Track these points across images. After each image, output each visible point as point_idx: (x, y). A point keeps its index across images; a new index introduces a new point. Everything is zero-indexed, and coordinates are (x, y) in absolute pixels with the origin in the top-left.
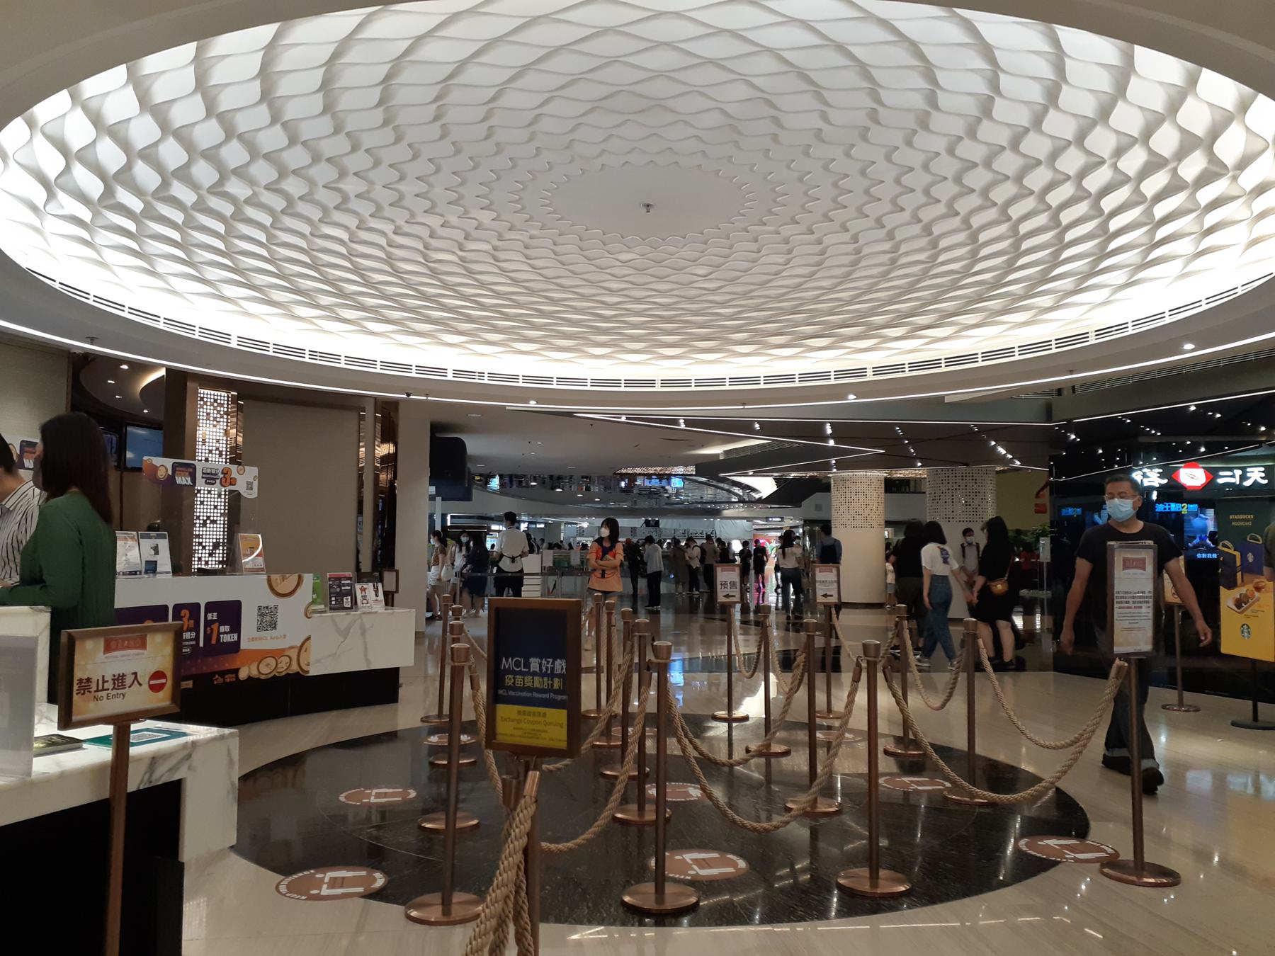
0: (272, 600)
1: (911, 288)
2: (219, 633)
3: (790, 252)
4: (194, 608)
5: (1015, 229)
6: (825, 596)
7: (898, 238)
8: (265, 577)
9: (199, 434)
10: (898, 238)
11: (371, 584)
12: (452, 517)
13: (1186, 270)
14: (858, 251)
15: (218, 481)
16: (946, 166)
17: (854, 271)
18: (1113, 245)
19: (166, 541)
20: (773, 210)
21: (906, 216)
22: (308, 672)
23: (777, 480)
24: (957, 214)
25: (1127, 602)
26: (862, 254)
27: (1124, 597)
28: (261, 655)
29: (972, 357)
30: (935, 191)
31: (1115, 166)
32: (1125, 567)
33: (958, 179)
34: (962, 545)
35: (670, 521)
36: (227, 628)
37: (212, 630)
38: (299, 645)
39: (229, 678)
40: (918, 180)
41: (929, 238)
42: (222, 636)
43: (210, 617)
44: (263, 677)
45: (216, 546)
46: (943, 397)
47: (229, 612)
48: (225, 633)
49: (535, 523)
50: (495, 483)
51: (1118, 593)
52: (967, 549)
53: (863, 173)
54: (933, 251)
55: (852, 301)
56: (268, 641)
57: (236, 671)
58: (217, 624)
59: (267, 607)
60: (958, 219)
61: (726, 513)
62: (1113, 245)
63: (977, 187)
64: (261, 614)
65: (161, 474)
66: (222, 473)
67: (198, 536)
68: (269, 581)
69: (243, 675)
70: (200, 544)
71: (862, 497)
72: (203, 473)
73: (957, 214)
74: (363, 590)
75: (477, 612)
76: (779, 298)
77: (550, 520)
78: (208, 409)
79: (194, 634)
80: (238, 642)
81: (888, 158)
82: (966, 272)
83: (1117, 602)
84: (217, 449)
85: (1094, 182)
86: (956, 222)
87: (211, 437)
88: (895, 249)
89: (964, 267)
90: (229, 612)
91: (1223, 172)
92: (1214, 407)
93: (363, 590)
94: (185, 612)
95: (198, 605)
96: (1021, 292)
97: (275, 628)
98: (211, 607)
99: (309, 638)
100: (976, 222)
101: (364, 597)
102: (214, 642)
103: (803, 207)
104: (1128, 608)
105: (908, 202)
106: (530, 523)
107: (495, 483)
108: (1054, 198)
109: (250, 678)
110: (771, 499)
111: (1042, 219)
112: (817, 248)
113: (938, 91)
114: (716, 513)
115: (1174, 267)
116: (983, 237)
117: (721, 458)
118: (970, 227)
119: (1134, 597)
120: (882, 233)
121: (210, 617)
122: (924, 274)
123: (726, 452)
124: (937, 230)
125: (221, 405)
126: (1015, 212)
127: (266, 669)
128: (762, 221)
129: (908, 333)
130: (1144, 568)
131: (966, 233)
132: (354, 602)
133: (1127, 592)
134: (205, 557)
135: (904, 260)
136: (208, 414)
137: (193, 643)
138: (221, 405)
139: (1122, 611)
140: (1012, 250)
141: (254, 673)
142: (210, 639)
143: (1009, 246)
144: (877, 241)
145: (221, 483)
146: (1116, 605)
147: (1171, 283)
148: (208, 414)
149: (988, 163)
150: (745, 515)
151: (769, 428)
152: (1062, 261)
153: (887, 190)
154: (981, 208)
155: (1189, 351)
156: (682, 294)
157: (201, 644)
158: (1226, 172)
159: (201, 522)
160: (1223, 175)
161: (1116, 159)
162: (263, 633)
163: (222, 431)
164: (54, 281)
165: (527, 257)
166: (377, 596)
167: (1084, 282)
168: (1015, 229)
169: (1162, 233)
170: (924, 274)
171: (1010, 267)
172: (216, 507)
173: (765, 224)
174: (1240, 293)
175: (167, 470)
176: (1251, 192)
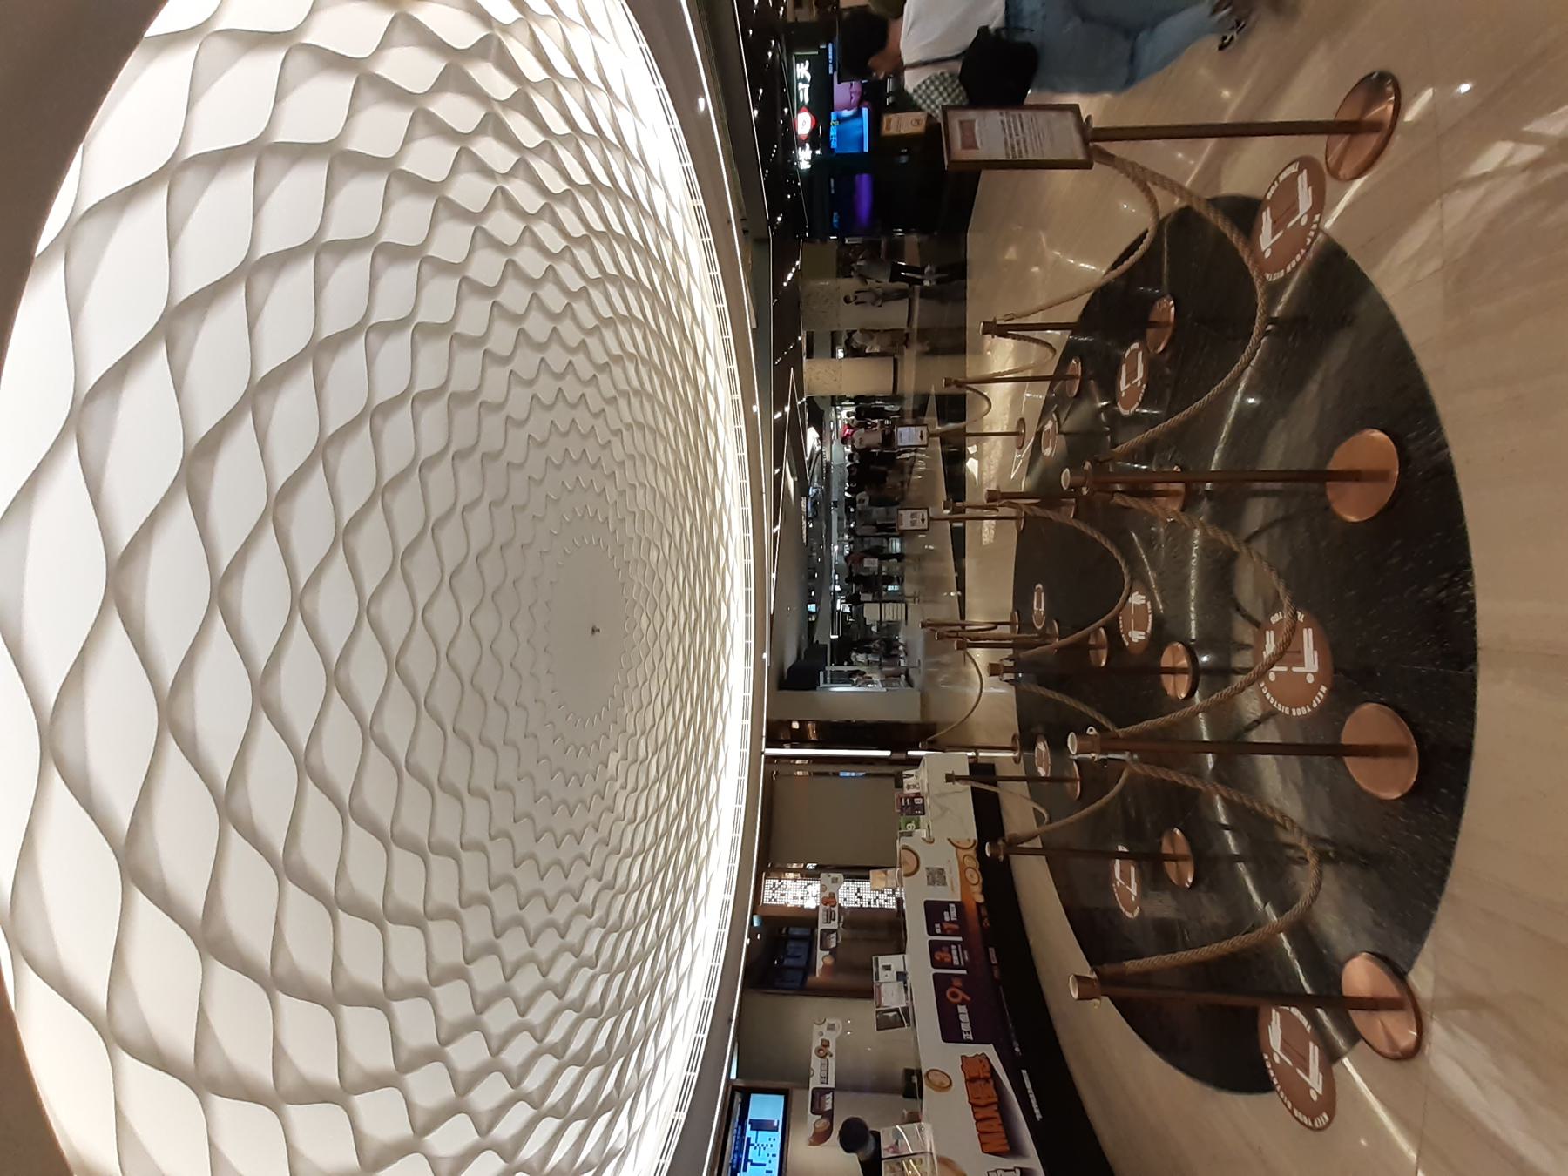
0: (922, 873)
1: (662, 373)
2: (951, 922)
3: (643, 458)
4: (934, 947)
5: (595, 282)
6: (922, 437)
7: (613, 393)
9: (792, 904)
10: (613, 393)
11: (904, 780)
12: (832, 634)
13: (625, 102)
14: (629, 427)
15: (833, 909)
16: (526, 362)
17: (648, 425)
18: (605, 180)
19: (880, 958)
20: (597, 491)
21: (590, 392)
22: (975, 841)
23: (809, 426)
24: (583, 341)
25: (1018, 143)
26: (632, 422)
27: (1013, 148)
28: (964, 881)
29: (719, 312)
30: (559, 367)
31: (507, 176)
32: (974, 146)
33: (542, 347)
34: (857, 303)
35: (833, 495)
36: (946, 913)
37: (949, 929)
38: (954, 848)
39: (984, 912)
40: (546, 389)
41: (611, 364)
43: (938, 931)
44: (981, 880)
46: (753, 330)
47: (934, 911)
49: (835, 581)
50: (812, 607)
51: (1007, 155)
52: (859, 300)
53: (543, 444)
54: (625, 359)
55: (676, 421)
56: (953, 876)
57: (978, 905)
58: (944, 924)
60: (589, 340)
61: (828, 459)
62: (605, 180)
63: (550, 326)
65: (829, 961)
66: (826, 905)
69: (980, 899)
70: (875, 901)
71: (820, 375)
72: (827, 922)
73: (583, 341)
74: (908, 787)
75: (902, 644)
76: (675, 483)
77: (834, 571)
78: (777, 895)
81: (522, 424)
82: (643, 325)
83: (1021, 156)
85: (531, 201)
86: (592, 343)
88: (625, 394)
89: (639, 328)
91: (495, 42)
92: (755, 93)
93: (908, 787)
95: (931, 942)
96: (660, 272)
97: (943, 870)
98: (931, 931)
99: (949, 840)
100: (589, 321)
102: (956, 927)
103: (594, 467)
104: (1025, 141)
105: (572, 392)
106: (835, 584)
107: (812, 607)
108: (555, 243)
109: (983, 892)
110: (820, 430)
111: (582, 255)
112: (628, 464)
113: (416, 391)
114: (828, 464)
115: (624, 117)
116: (606, 313)
117: (796, 479)
118: (596, 328)
119: (1011, 136)
120: (609, 410)
121: (938, 931)
122: (648, 363)
123: (792, 475)
124: (602, 358)
125: (774, 885)
126: (575, 283)
127: (975, 878)
128: (603, 523)
129: (701, 369)
130: (972, 122)
131: (603, 330)
132: (918, 795)
133: (1006, 143)
135: (636, 383)
136: (782, 895)
137: (959, 946)
138: (774, 885)
139: (1030, 151)
140: (619, 284)
141: (977, 889)
143: (615, 286)
144: (618, 412)
145: (834, 906)
146: (1024, 158)
147: (641, 121)
148: (782, 895)
149: (517, 318)
150: (829, 446)
151: (778, 463)
152: (625, 233)
153: (562, 416)
154: (574, 318)
155: (704, 103)
156: (665, 608)
157: (960, 939)
158: (495, 42)
160: (500, 43)
161: (497, 176)
165: (635, 790)
166: (912, 776)
167: (646, 211)
168: (595, 282)
169: (587, 127)
170: (648, 363)
171: (636, 284)
173: (607, 518)
174: (646, 44)
175: (825, 956)
176: (521, 12)
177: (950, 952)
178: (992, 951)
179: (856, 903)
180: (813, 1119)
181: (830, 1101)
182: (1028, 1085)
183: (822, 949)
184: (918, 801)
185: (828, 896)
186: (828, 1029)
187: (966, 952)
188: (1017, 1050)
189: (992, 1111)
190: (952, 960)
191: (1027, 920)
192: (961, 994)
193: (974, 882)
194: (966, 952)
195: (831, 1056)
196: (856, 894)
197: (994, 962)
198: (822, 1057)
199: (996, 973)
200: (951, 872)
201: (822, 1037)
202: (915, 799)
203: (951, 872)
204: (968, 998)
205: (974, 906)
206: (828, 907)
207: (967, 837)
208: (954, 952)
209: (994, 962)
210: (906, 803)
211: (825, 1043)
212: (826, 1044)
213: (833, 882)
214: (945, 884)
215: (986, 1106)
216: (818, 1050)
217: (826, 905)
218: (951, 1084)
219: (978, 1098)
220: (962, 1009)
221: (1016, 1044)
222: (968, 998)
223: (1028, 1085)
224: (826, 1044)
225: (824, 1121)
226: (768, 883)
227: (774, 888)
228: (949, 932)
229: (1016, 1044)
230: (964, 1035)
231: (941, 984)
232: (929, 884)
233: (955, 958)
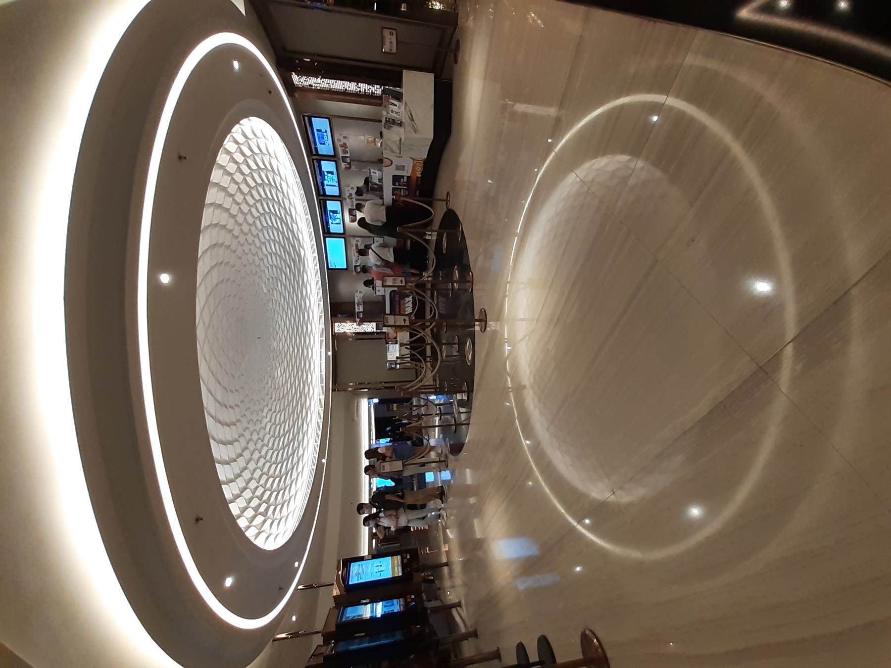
0: (394, 166)
8: (384, 168)
38: (412, 160)
39: (420, 179)
44: (422, 170)
57: (417, 177)
64: (398, 169)
67: (365, 90)
79: (402, 190)
80: (407, 176)
90: (396, 179)
94: (395, 192)
95: (393, 188)
98: (394, 184)
101: (397, 113)
109: (421, 174)
121: (397, 185)
157: (406, 187)
162: (406, 170)
177: (401, 191)
205: (416, 177)
207: (420, 157)
214: (404, 170)
216: (348, 197)
224: (351, 195)
232: (396, 169)
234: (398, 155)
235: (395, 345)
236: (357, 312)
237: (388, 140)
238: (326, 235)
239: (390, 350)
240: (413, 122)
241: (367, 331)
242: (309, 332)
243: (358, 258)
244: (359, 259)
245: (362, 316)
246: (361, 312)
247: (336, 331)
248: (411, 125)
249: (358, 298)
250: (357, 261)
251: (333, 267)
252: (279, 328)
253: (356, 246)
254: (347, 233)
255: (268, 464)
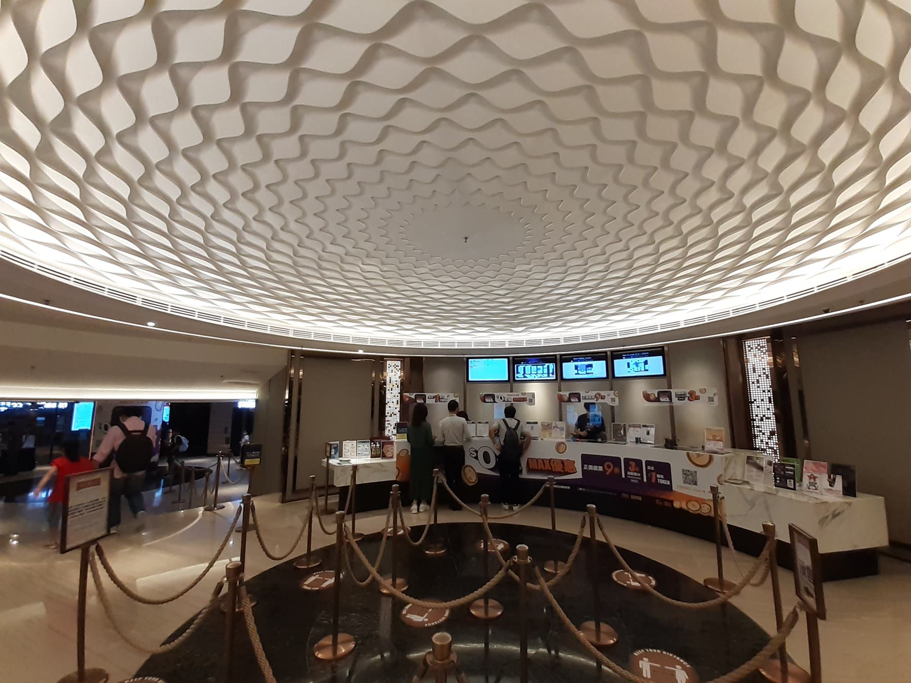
0: (693, 468)
4: (638, 462)
15: (687, 398)
28: (689, 499)
36: (662, 477)
37: (651, 475)
39: (666, 504)
42: (658, 479)
44: (691, 512)
45: (772, 433)
48: (660, 478)
57: (672, 502)
58: (654, 474)
59: (689, 471)
66: (689, 393)
68: (688, 455)
72: (676, 395)
79: (639, 475)
84: (764, 373)
87: (759, 367)
98: (648, 463)
102: (653, 480)
109: (681, 509)
134: (766, 440)
137: (640, 478)
141: (684, 507)
142: (651, 479)
145: (689, 399)
157: (645, 480)
159: (760, 418)
163: (751, 361)
164: (883, 264)
172: (758, 407)
175: (655, 395)
178: (640, 498)
179: (757, 416)
180: (567, 394)
181: (490, 401)
182: (562, 487)
183: (569, 394)
184: (790, 483)
185: (697, 395)
186: (612, 399)
187: (636, 481)
188: (581, 489)
189: (548, 467)
190: (630, 471)
191: (663, 532)
192: (609, 471)
193: (698, 507)
194: (636, 481)
195: (596, 400)
196: (393, 413)
197: (633, 497)
198: (595, 396)
199: (625, 495)
200: (694, 490)
201: (606, 396)
202: (792, 481)
203: (694, 490)
204: (608, 473)
205: (671, 498)
206: (688, 395)
208: (636, 474)
209: (633, 497)
210: (788, 470)
211: (525, 399)
212: (603, 398)
213: (709, 398)
215: (551, 466)
216: (599, 394)
217: (689, 393)
218: (559, 452)
219: (554, 462)
220: (601, 468)
221: (584, 490)
222: (608, 473)
223: (562, 487)
224: (603, 398)
225: (567, 399)
226: (763, 342)
227: (759, 347)
228: (649, 475)
229: (584, 490)
230: (586, 465)
231: (616, 461)
233: (632, 474)
234: (723, 478)
235: (368, 453)
236: (425, 396)
237: (735, 461)
238: (511, 358)
239: (361, 445)
240: (830, 517)
241: (387, 406)
242: (439, 327)
243: (506, 400)
244: (504, 401)
245: (418, 401)
246: (425, 401)
247: (388, 362)
248: (826, 515)
249: (446, 397)
250: (501, 398)
251: (470, 365)
252: (427, 285)
253: (523, 398)
254: (515, 385)
255: (208, 210)
